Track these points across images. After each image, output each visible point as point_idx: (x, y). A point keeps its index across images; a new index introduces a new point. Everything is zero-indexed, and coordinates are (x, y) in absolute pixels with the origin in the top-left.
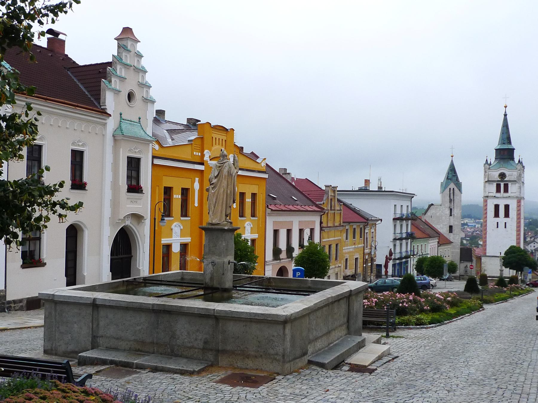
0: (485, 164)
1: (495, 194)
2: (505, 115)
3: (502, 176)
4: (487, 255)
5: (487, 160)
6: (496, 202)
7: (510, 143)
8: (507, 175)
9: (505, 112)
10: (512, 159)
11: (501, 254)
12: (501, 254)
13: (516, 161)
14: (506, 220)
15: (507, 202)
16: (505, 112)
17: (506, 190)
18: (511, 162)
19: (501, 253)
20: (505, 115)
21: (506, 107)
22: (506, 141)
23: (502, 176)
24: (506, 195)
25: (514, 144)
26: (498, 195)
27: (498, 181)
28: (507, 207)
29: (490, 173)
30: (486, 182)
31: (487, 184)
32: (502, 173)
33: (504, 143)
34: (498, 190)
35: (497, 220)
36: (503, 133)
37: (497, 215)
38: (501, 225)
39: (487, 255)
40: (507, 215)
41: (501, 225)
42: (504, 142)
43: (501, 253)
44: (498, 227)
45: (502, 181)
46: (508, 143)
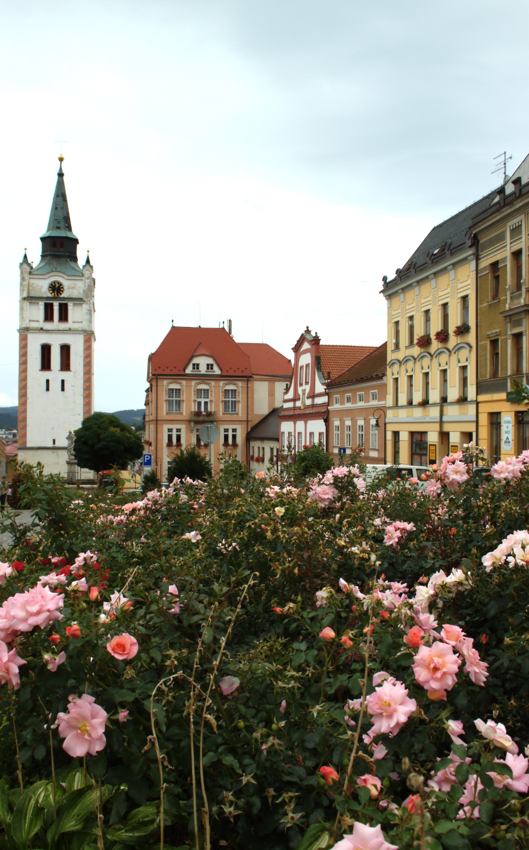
0: (21, 264)
1: (42, 324)
2: (61, 175)
3: (56, 288)
4: (29, 445)
5: (25, 257)
6: (45, 339)
7: (69, 228)
8: (65, 287)
9: (61, 169)
10: (74, 259)
11: (54, 443)
12: (54, 443)
13: (81, 262)
14: (65, 375)
15: (66, 339)
16: (61, 169)
17: (64, 317)
18: (73, 264)
19: (54, 441)
20: (61, 175)
21: (61, 160)
22: (62, 224)
23: (56, 288)
24: (63, 326)
25: (77, 231)
26: (48, 326)
27: (48, 298)
28: (65, 350)
29: (32, 281)
30: (24, 299)
31: (26, 304)
32: (54, 282)
33: (58, 228)
34: (48, 317)
35: (47, 375)
36: (56, 208)
37: (46, 365)
38: (55, 385)
39: (29, 445)
40: (66, 366)
41: (55, 385)
42: (59, 225)
43: (54, 441)
44: (48, 389)
45: (55, 298)
46: (66, 227)
